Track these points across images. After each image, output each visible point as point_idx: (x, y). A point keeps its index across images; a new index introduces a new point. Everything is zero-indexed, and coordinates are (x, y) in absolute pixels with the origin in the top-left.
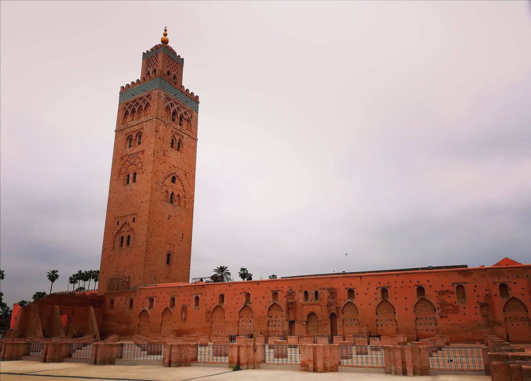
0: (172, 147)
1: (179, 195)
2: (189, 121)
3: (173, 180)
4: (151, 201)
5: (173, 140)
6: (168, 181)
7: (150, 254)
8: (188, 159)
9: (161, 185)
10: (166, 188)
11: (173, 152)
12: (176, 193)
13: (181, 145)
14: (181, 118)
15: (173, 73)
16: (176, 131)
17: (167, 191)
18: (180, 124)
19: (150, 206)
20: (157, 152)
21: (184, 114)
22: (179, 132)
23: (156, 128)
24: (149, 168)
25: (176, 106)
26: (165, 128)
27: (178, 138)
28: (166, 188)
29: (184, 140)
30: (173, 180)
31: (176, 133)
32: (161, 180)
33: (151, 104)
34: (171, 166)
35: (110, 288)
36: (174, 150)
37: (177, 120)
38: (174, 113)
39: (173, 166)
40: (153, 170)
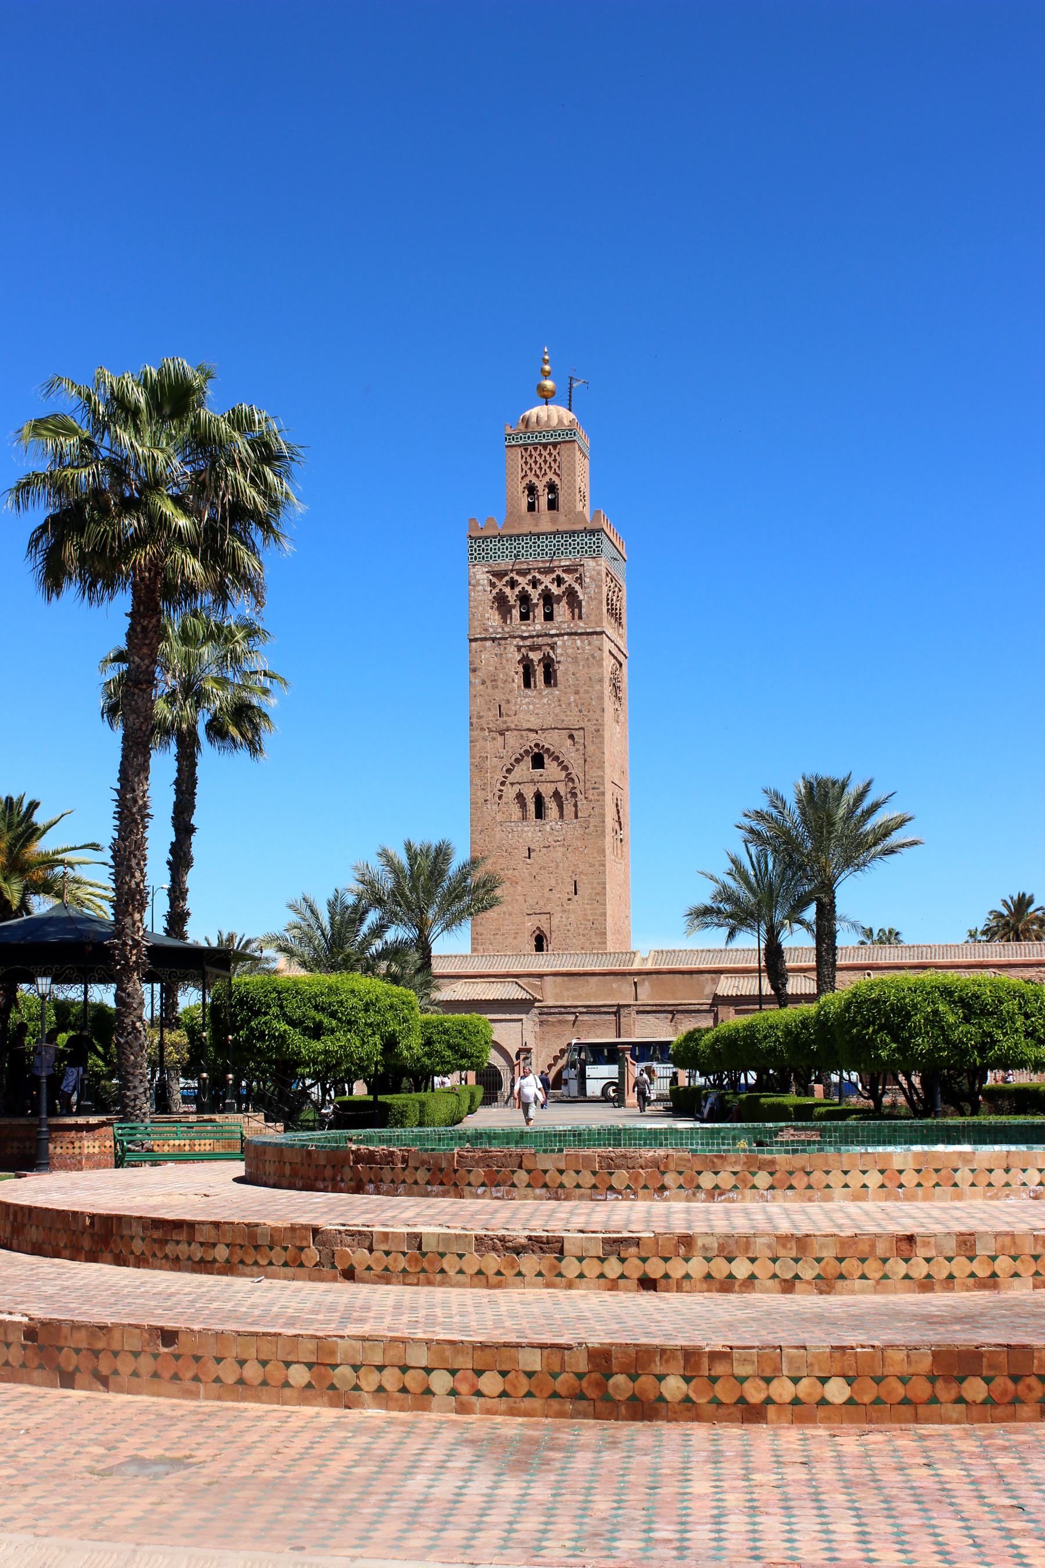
0: (527, 685)
1: (556, 795)
2: (571, 596)
3: (538, 762)
6: (524, 770)
8: (577, 693)
10: (517, 788)
12: (547, 791)
14: (548, 599)
15: (541, 485)
16: (528, 643)
17: (520, 797)
18: (549, 617)
20: (480, 717)
26: (497, 650)
27: (535, 656)
28: (517, 788)
29: (559, 651)
30: (538, 762)
31: (533, 648)
39: (530, 730)
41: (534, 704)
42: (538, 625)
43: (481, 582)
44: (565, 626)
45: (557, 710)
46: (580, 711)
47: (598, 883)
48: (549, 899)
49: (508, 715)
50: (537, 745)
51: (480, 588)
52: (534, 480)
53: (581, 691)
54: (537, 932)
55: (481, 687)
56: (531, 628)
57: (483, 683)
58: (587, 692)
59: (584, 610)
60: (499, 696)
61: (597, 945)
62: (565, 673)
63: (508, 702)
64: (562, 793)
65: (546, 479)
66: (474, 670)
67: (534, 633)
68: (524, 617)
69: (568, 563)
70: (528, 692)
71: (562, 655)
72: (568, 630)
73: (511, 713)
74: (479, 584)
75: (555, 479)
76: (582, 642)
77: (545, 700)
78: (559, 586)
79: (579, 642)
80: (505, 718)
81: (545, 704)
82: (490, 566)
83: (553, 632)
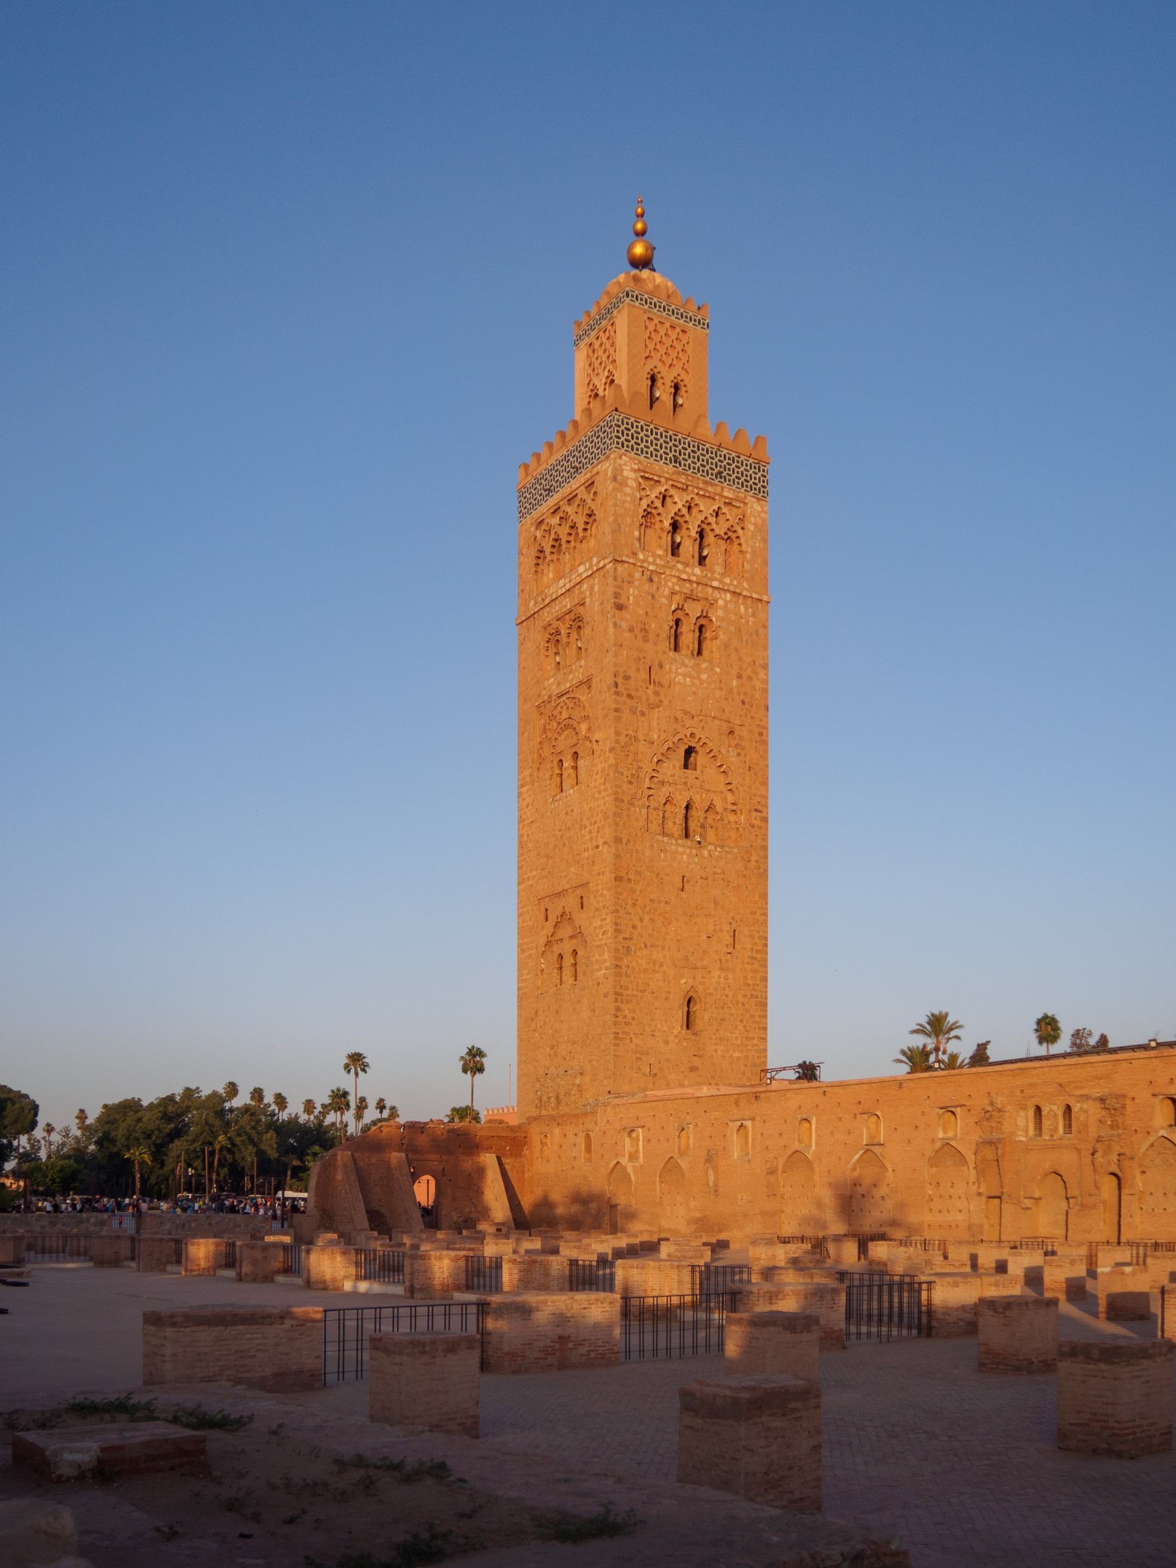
4: (618, 840)
5: (677, 622)
6: (673, 767)
7: (628, 1002)
9: (647, 783)
10: (666, 790)
11: (683, 664)
13: (708, 634)
15: (667, 378)
19: (618, 856)
20: (627, 678)
22: (700, 591)
24: (604, 735)
28: (666, 790)
31: (687, 598)
32: (648, 767)
33: (599, 514)
34: (679, 714)
35: (540, 1104)
37: (689, 549)
39: (686, 713)
40: (617, 742)
41: (692, 678)
44: (727, 580)
45: (718, 694)
47: (759, 938)
48: (705, 952)
50: (692, 735)
52: (660, 367)
54: (690, 994)
56: (689, 570)
57: (631, 630)
61: (757, 1019)
62: (726, 646)
63: (661, 666)
64: (719, 808)
65: (674, 372)
67: (694, 579)
69: (731, 496)
71: (723, 619)
72: (732, 588)
73: (664, 682)
75: (683, 375)
77: (704, 677)
80: (657, 689)
81: (702, 682)
83: (715, 584)
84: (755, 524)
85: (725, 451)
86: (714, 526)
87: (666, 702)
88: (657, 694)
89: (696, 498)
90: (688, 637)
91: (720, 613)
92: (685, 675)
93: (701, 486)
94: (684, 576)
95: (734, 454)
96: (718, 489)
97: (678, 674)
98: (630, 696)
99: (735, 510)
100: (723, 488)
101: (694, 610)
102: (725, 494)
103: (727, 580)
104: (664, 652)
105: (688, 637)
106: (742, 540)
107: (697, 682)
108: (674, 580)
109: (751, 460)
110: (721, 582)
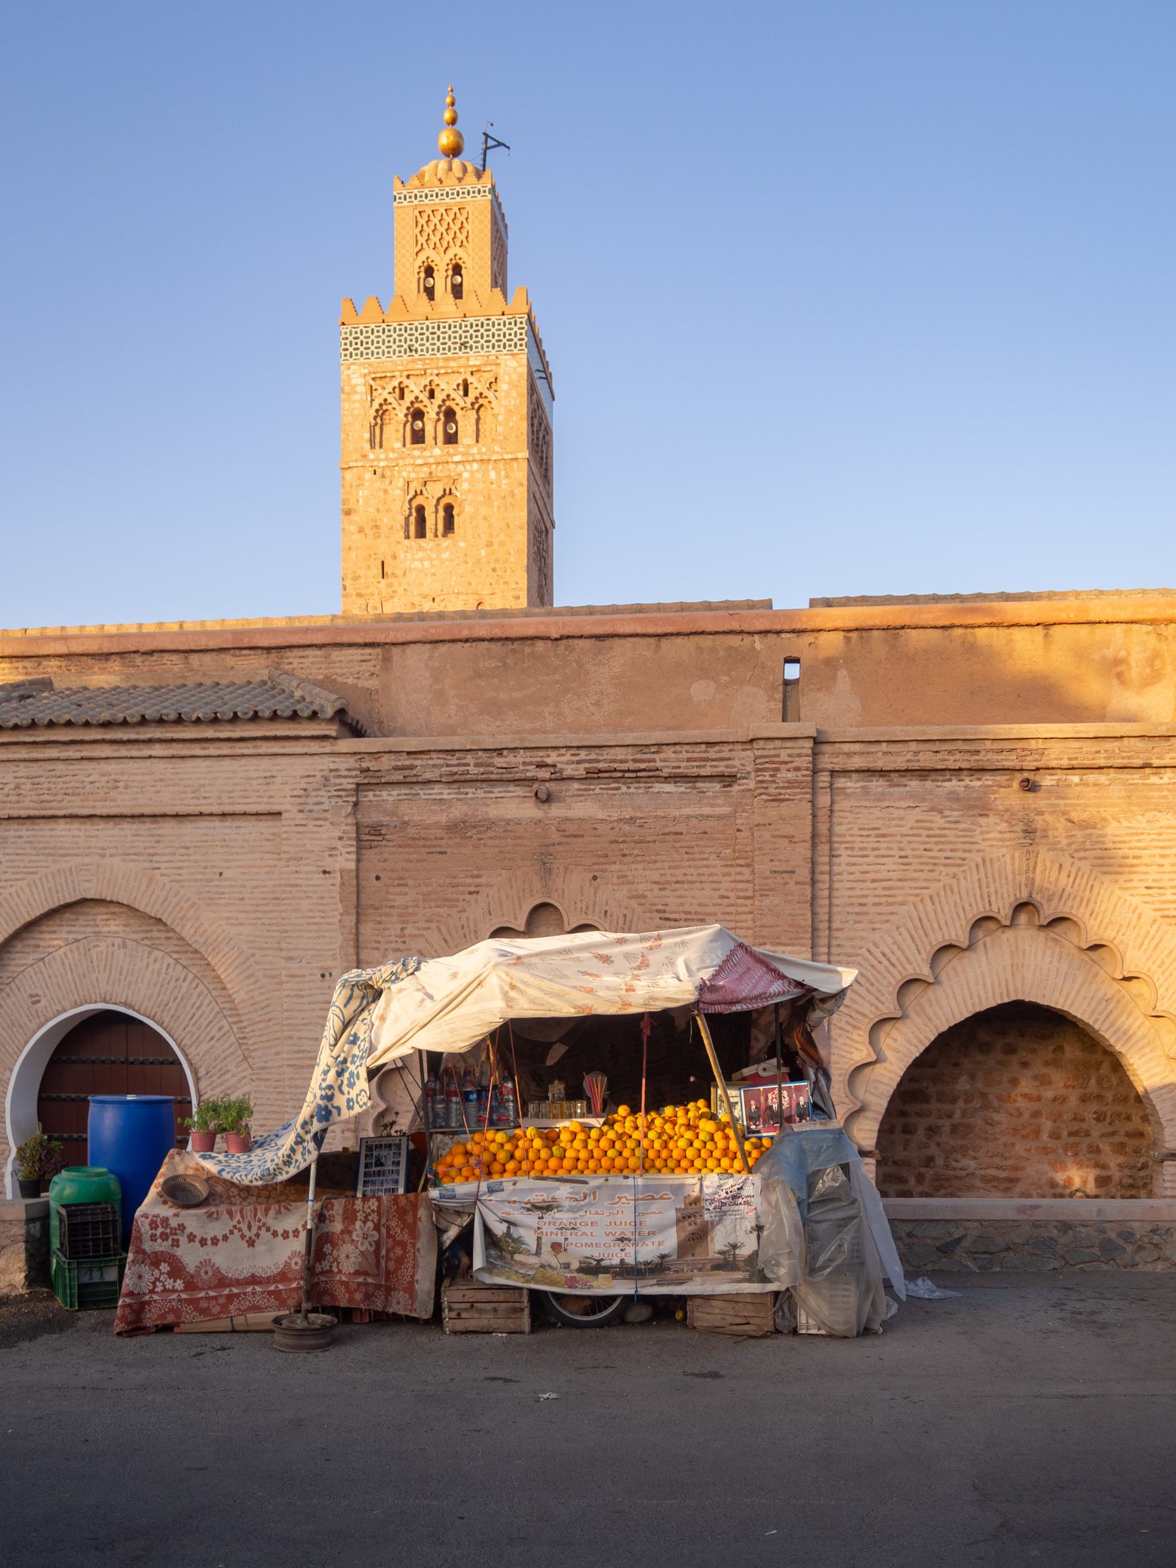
8: (489, 544)
11: (421, 548)
20: (356, 578)
21: (458, 396)
22: (439, 471)
23: (345, 502)
25: (415, 389)
26: (378, 484)
29: (465, 486)
36: (427, 543)
38: (418, 415)
41: (431, 560)
42: (435, 450)
43: (359, 389)
44: (475, 450)
46: (494, 570)
49: (395, 576)
51: (357, 397)
53: (496, 541)
55: (357, 537)
56: (427, 453)
58: (502, 543)
59: (500, 429)
60: (383, 548)
63: (395, 557)
66: (348, 513)
67: (431, 461)
68: (418, 437)
69: (478, 363)
70: (421, 541)
72: (478, 457)
73: (399, 572)
74: (356, 393)
76: (498, 474)
77: (445, 555)
78: (466, 394)
79: (493, 474)
81: (442, 561)
82: (370, 365)
83: (458, 458)
84: (510, 383)
85: (472, 320)
86: (459, 400)
87: (400, 591)
88: (390, 585)
89: (435, 378)
90: (434, 520)
91: (465, 486)
92: (422, 560)
93: (441, 364)
94: (420, 462)
95: (483, 319)
96: (463, 361)
97: (414, 560)
98: (359, 595)
99: (486, 374)
100: (468, 359)
101: (435, 490)
102: (471, 363)
103: (475, 450)
104: (399, 543)
105: (434, 520)
106: (494, 402)
107: (437, 562)
108: (410, 468)
109: (504, 318)
110: (463, 454)
